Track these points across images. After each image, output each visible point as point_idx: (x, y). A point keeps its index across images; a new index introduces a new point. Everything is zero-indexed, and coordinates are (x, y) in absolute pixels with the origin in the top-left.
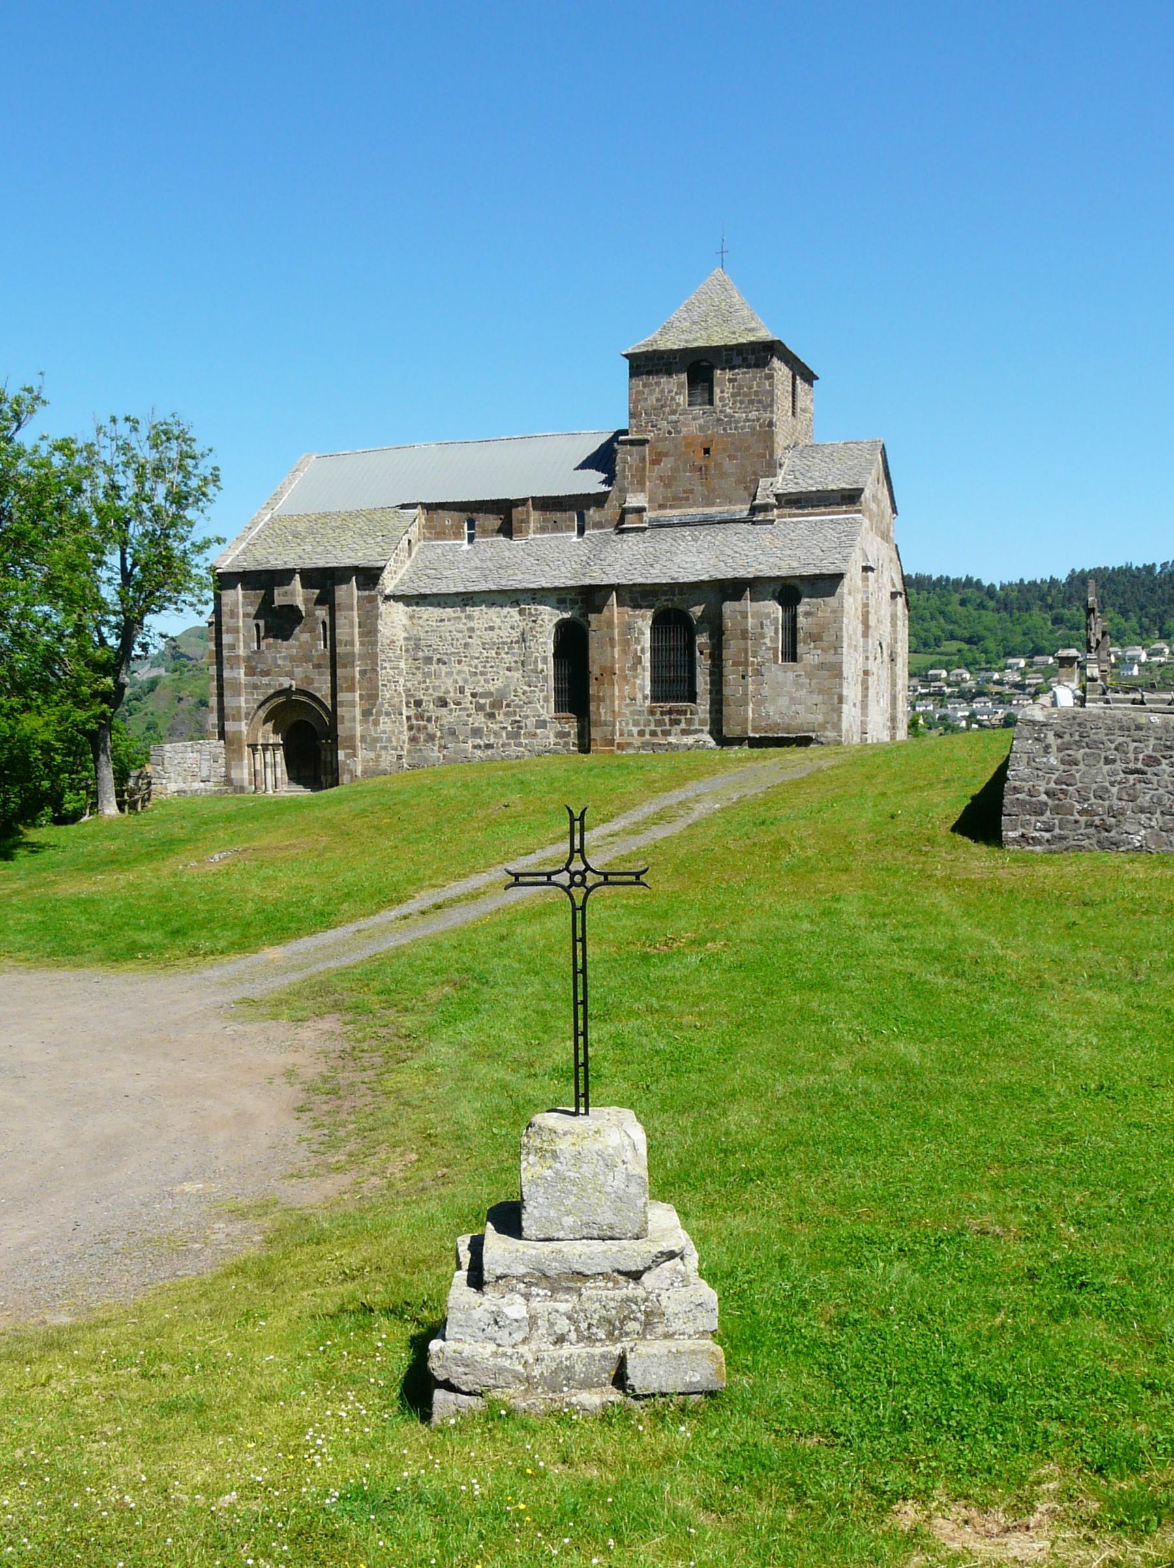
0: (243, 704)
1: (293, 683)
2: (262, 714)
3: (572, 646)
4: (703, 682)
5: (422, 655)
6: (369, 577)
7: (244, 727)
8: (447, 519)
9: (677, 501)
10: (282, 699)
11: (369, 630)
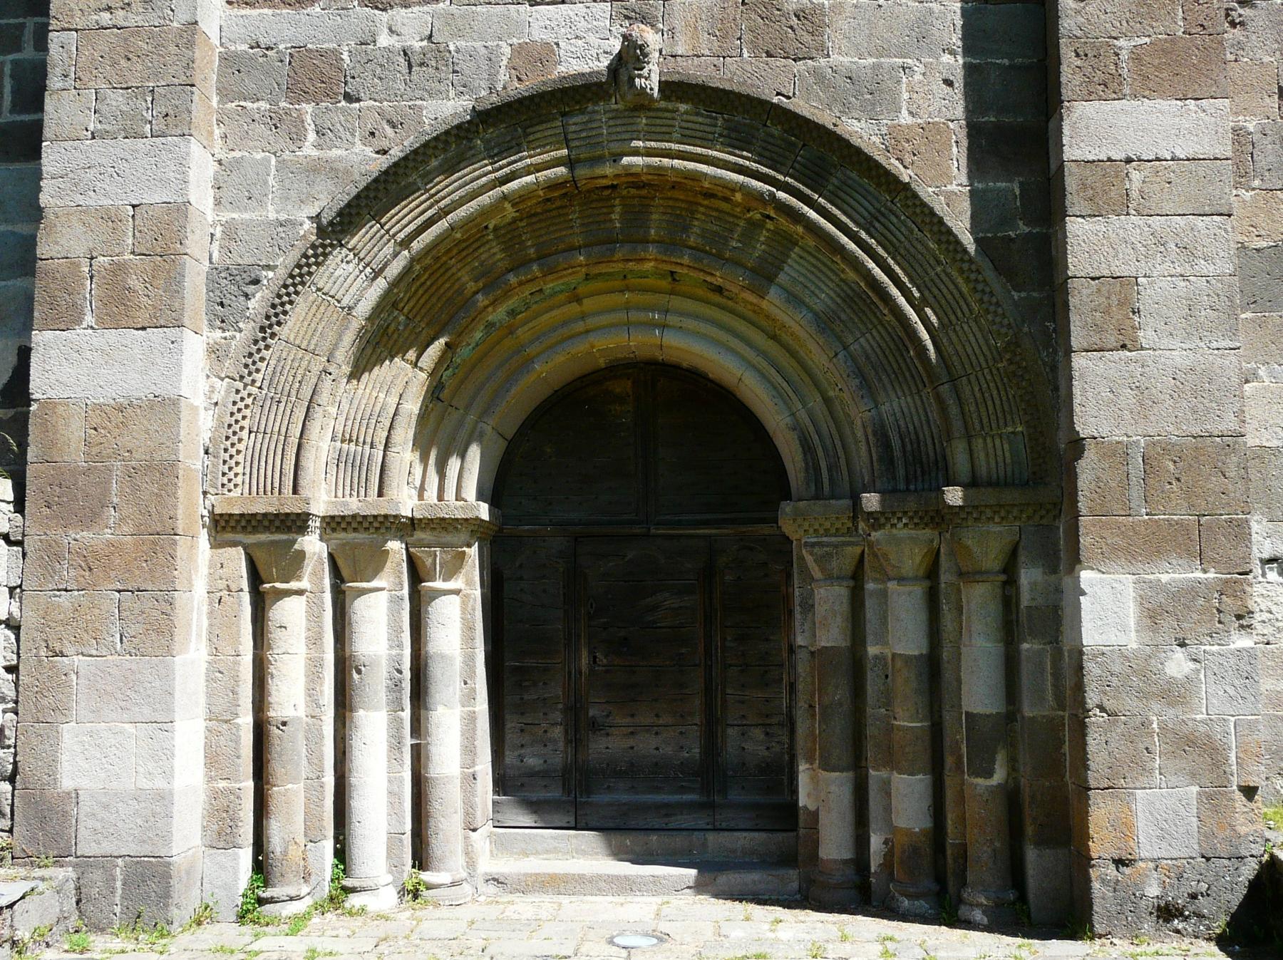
0: (201, 197)
1: (651, 38)
2: (355, 282)
7: (192, 370)
10: (536, 169)
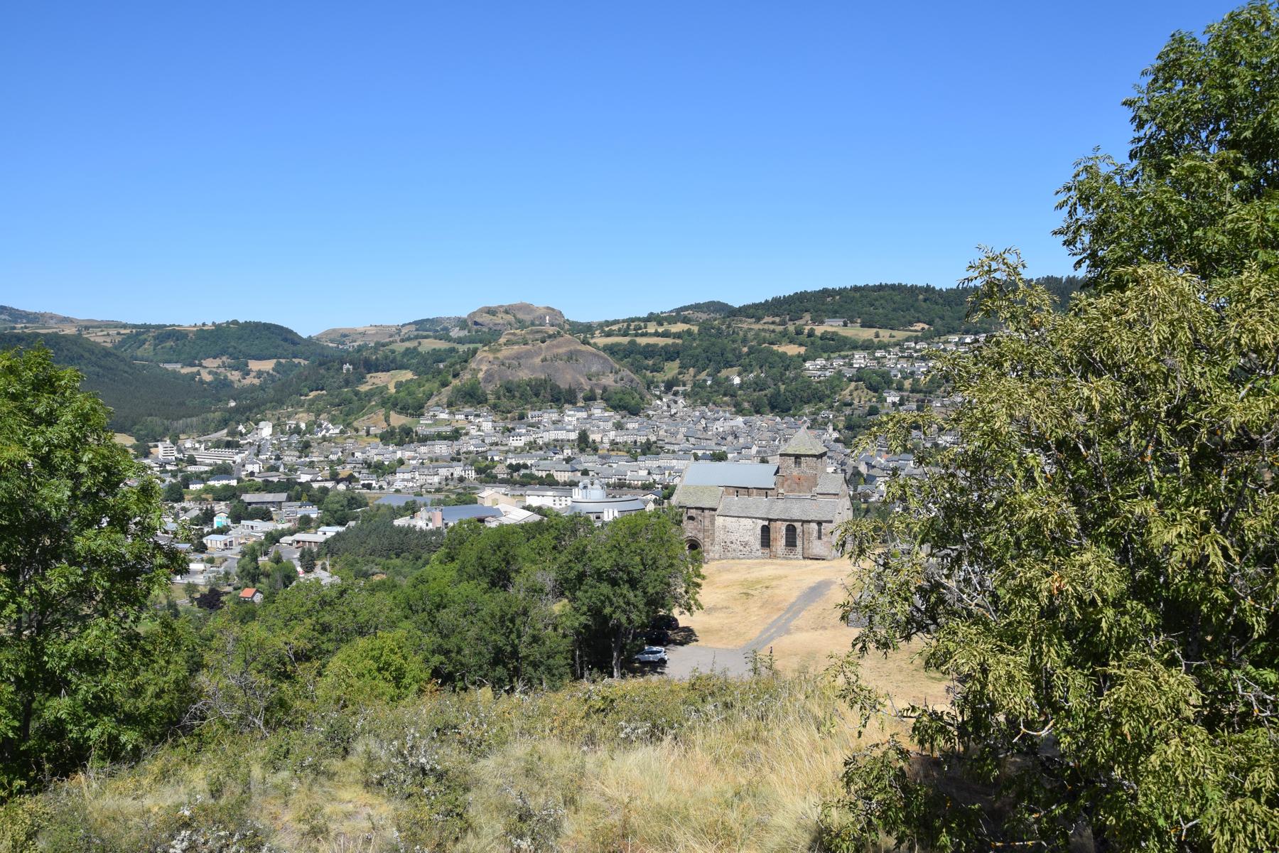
3: (766, 530)
4: (799, 543)
5: (727, 530)
6: (714, 510)
8: (731, 490)
9: (792, 491)
11: (712, 522)
